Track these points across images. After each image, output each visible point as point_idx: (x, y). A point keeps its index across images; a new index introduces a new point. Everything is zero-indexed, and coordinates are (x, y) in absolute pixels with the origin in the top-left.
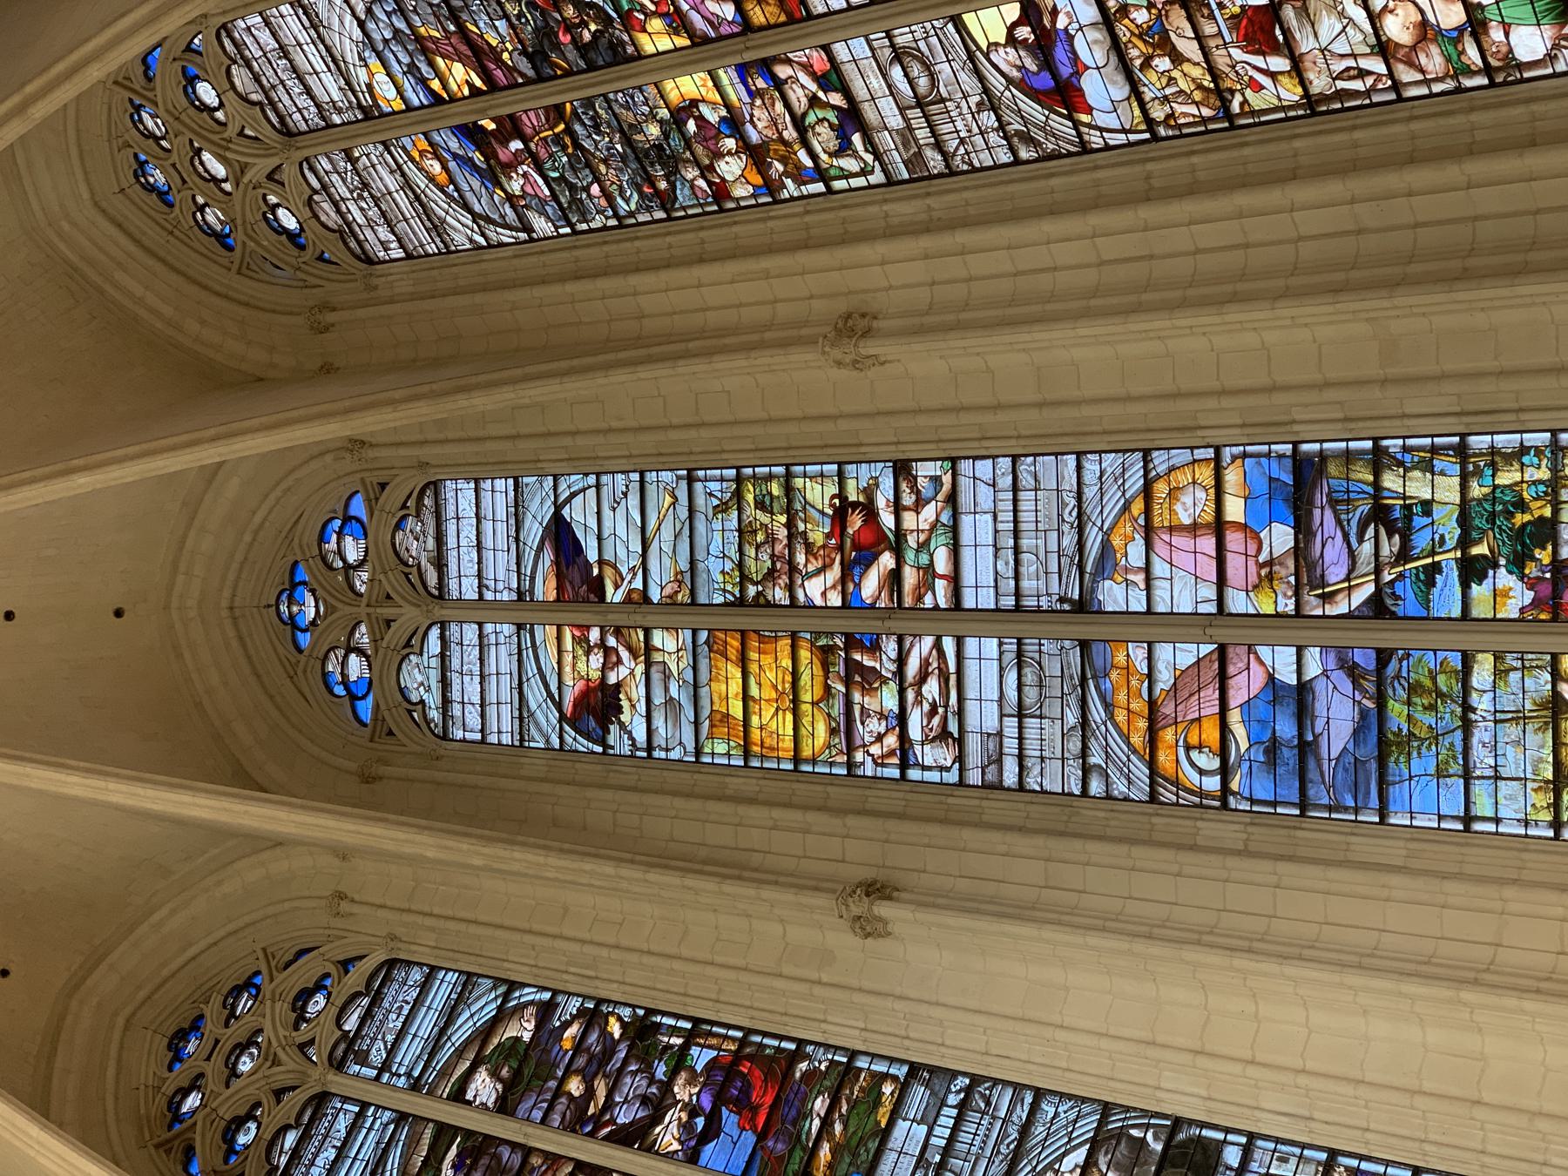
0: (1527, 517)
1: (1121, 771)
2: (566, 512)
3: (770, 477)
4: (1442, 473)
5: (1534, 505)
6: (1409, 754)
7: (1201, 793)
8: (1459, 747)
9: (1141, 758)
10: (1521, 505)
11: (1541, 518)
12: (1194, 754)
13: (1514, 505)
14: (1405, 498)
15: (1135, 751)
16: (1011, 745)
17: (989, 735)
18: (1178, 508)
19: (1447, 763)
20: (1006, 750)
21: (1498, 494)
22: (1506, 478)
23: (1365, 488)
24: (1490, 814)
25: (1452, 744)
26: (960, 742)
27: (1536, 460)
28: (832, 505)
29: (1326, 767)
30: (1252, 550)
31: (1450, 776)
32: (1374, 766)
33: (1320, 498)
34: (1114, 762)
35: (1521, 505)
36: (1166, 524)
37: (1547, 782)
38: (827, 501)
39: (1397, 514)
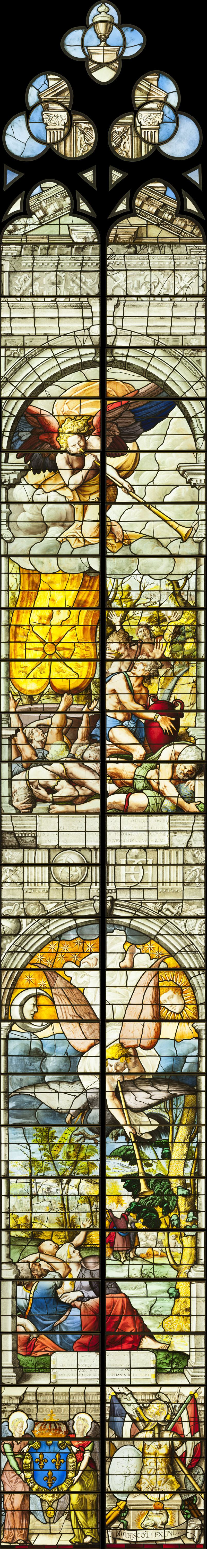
0: (160, 1215)
1: (19, 946)
2: (176, 412)
3: (197, 642)
4: (185, 1165)
5: (167, 1218)
6: (42, 1143)
7: (9, 1005)
8: (47, 1173)
9: (28, 962)
10: (167, 1212)
11: (160, 1223)
12: (32, 1001)
13: (168, 1206)
14: (173, 1142)
15: (32, 956)
16: (30, 856)
17: (36, 837)
18: (170, 992)
19: (38, 1166)
20: (26, 852)
21: (173, 1198)
22: (181, 1201)
23: (179, 1119)
24: (12, 1191)
25: (48, 1169)
26: (30, 812)
27: (191, 1219)
28: (177, 701)
29: (31, 1090)
30: (145, 1043)
31: (31, 1167)
32: (33, 1121)
33: (174, 1090)
34: (24, 941)
35: (167, 1212)
36: (161, 984)
37: (31, 1225)
38: (179, 697)
39: (163, 1138)
